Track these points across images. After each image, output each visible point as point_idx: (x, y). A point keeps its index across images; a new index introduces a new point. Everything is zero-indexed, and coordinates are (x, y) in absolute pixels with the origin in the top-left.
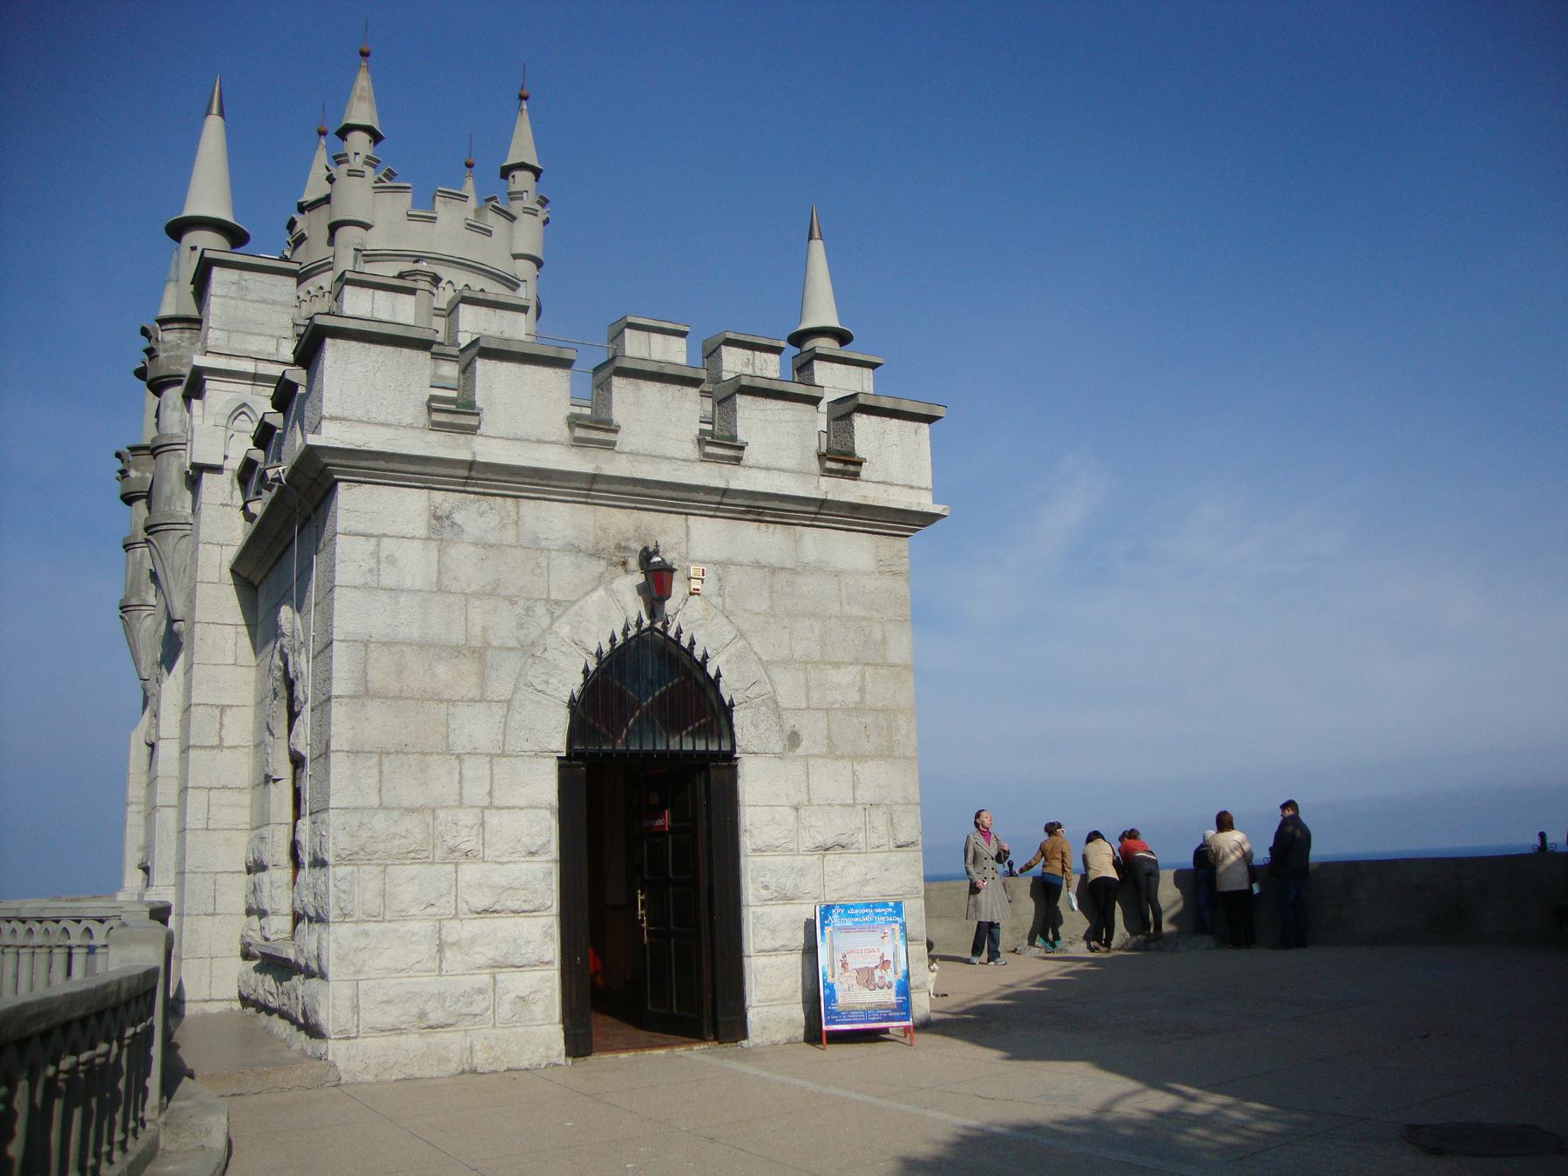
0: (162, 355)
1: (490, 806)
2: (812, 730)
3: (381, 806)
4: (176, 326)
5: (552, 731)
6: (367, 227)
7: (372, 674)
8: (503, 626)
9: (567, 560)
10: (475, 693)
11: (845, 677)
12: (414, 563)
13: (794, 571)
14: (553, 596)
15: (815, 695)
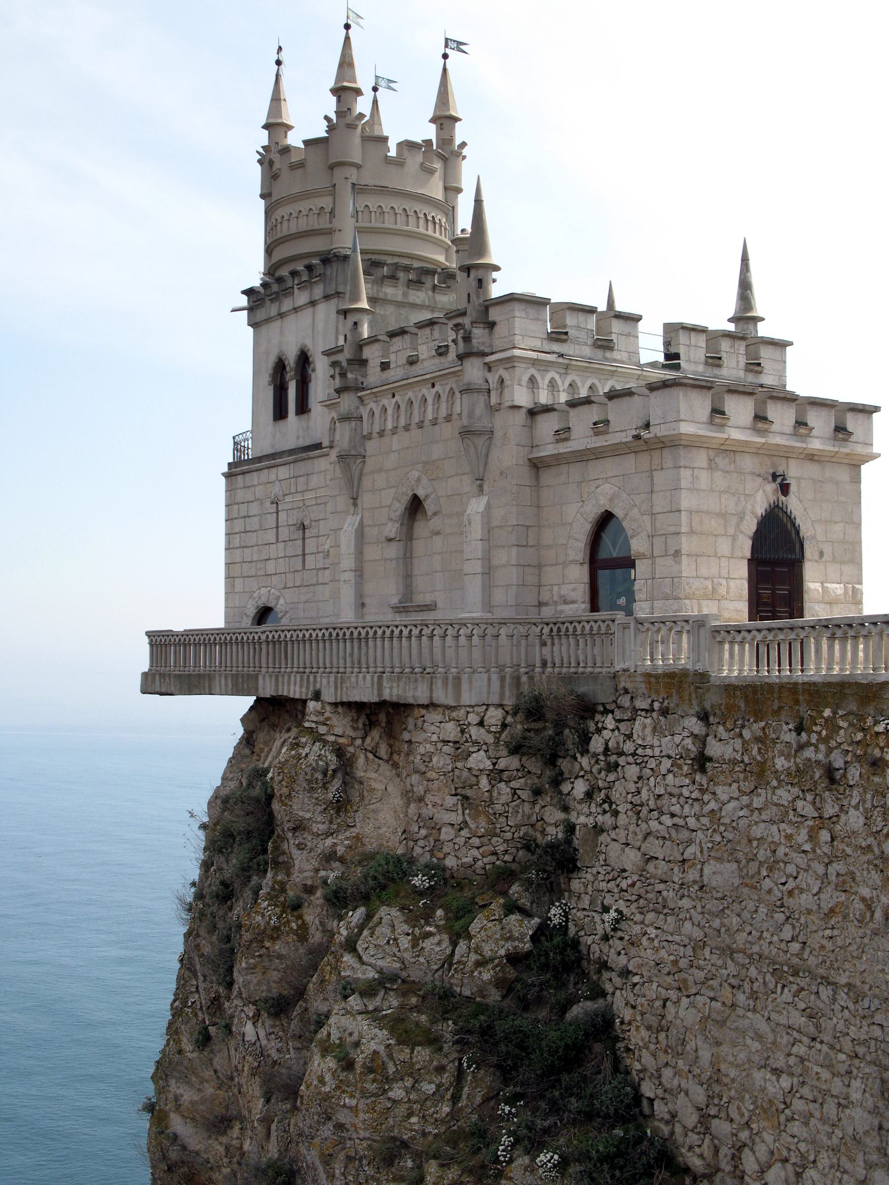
0: (474, 341)
1: (728, 578)
2: (827, 549)
3: (697, 577)
4: (482, 326)
5: (746, 547)
6: (358, 167)
7: (693, 524)
8: (729, 504)
9: (749, 477)
10: (723, 532)
11: (838, 528)
12: (704, 477)
13: (823, 482)
14: (747, 492)
15: (829, 535)
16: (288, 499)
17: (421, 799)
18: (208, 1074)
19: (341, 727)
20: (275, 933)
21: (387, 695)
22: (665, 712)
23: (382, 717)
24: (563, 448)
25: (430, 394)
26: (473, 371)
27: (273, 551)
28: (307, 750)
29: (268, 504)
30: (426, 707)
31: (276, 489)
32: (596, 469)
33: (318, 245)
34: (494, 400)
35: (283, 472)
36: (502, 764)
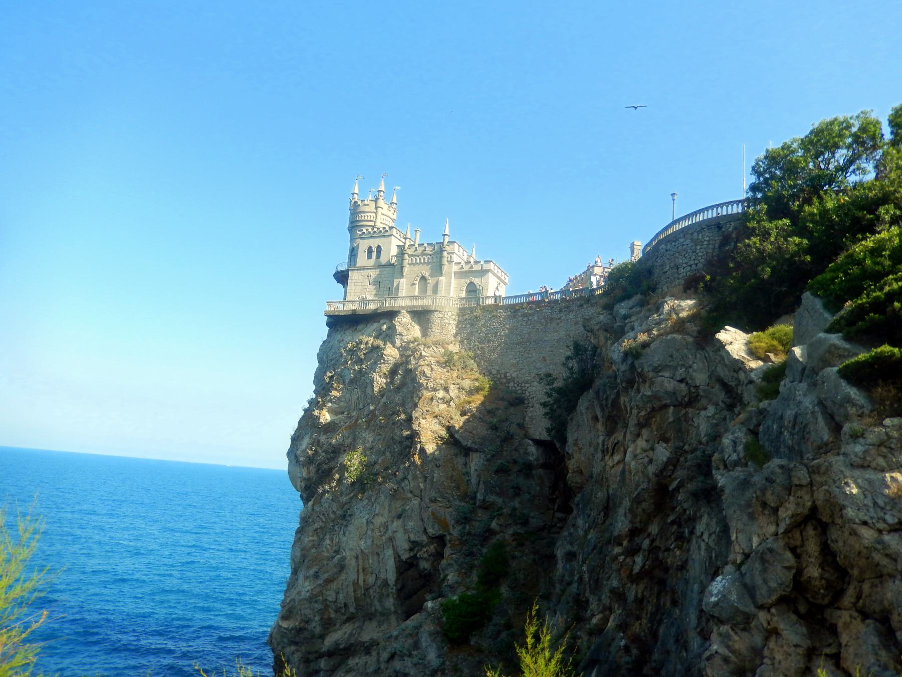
33: (372, 224)
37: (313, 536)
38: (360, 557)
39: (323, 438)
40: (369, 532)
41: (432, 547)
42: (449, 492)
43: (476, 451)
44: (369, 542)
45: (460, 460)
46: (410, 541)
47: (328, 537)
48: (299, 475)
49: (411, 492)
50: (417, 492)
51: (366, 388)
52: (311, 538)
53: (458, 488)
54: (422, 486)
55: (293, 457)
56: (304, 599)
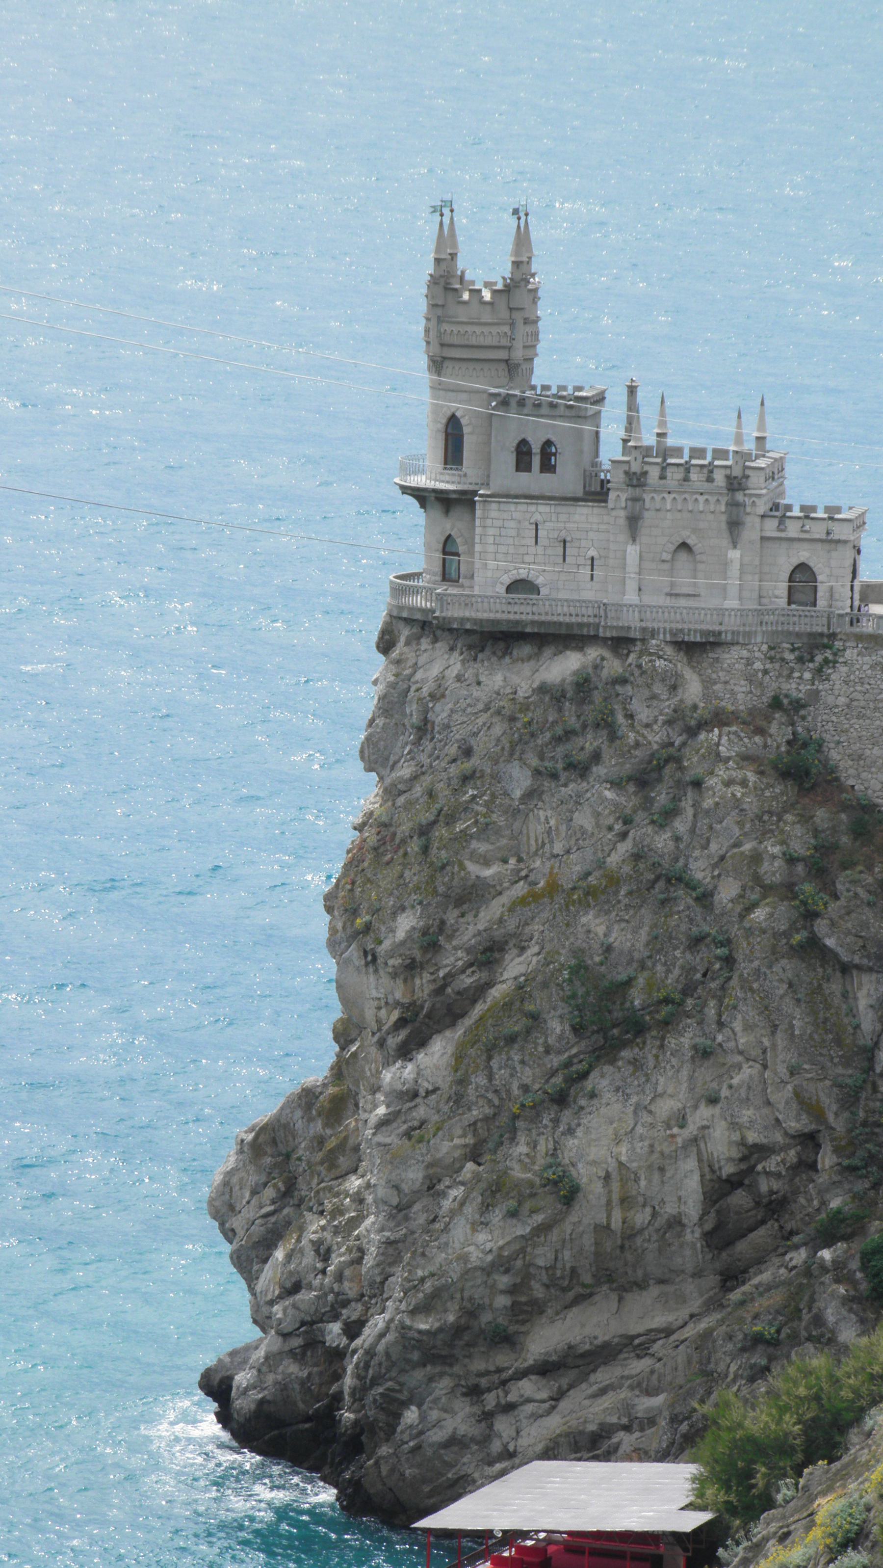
16: (547, 524)
17: (726, 683)
18: (508, 832)
19: (669, 651)
20: (637, 745)
21: (711, 639)
22: (866, 649)
23: (683, 646)
24: (783, 535)
25: (701, 499)
26: (739, 497)
27: (532, 550)
28: (657, 663)
29: (527, 523)
30: (733, 644)
31: (537, 517)
32: (796, 545)
33: (502, 355)
34: (748, 509)
35: (542, 508)
36: (767, 666)
37: (464, 1136)
38: (615, 1175)
39: (451, 916)
40: (640, 1130)
41: (792, 1153)
42: (824, 1051)
43: (871, 970)
44: (641, 1147)
45: (835, 987)
46: (743, 1143)
47: (522, 1138)
48: (374, 994)
49: (741, 1053)
50: (755, 1052)
51: (572, 812)
52: (457, 1141)
53: (838, 1042)
54: (766, 1042)
55: (353, 952)
56: (475, 1268)
